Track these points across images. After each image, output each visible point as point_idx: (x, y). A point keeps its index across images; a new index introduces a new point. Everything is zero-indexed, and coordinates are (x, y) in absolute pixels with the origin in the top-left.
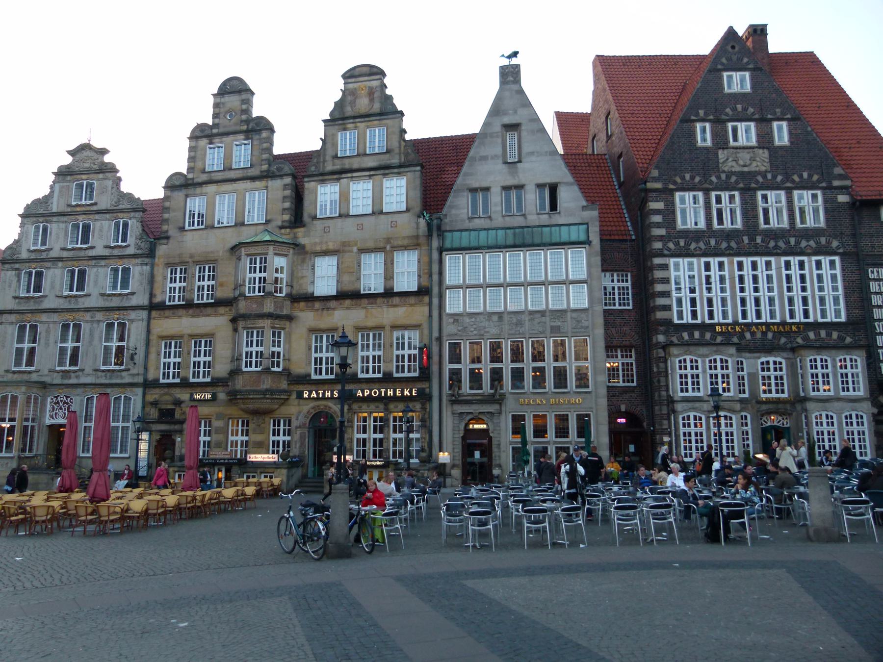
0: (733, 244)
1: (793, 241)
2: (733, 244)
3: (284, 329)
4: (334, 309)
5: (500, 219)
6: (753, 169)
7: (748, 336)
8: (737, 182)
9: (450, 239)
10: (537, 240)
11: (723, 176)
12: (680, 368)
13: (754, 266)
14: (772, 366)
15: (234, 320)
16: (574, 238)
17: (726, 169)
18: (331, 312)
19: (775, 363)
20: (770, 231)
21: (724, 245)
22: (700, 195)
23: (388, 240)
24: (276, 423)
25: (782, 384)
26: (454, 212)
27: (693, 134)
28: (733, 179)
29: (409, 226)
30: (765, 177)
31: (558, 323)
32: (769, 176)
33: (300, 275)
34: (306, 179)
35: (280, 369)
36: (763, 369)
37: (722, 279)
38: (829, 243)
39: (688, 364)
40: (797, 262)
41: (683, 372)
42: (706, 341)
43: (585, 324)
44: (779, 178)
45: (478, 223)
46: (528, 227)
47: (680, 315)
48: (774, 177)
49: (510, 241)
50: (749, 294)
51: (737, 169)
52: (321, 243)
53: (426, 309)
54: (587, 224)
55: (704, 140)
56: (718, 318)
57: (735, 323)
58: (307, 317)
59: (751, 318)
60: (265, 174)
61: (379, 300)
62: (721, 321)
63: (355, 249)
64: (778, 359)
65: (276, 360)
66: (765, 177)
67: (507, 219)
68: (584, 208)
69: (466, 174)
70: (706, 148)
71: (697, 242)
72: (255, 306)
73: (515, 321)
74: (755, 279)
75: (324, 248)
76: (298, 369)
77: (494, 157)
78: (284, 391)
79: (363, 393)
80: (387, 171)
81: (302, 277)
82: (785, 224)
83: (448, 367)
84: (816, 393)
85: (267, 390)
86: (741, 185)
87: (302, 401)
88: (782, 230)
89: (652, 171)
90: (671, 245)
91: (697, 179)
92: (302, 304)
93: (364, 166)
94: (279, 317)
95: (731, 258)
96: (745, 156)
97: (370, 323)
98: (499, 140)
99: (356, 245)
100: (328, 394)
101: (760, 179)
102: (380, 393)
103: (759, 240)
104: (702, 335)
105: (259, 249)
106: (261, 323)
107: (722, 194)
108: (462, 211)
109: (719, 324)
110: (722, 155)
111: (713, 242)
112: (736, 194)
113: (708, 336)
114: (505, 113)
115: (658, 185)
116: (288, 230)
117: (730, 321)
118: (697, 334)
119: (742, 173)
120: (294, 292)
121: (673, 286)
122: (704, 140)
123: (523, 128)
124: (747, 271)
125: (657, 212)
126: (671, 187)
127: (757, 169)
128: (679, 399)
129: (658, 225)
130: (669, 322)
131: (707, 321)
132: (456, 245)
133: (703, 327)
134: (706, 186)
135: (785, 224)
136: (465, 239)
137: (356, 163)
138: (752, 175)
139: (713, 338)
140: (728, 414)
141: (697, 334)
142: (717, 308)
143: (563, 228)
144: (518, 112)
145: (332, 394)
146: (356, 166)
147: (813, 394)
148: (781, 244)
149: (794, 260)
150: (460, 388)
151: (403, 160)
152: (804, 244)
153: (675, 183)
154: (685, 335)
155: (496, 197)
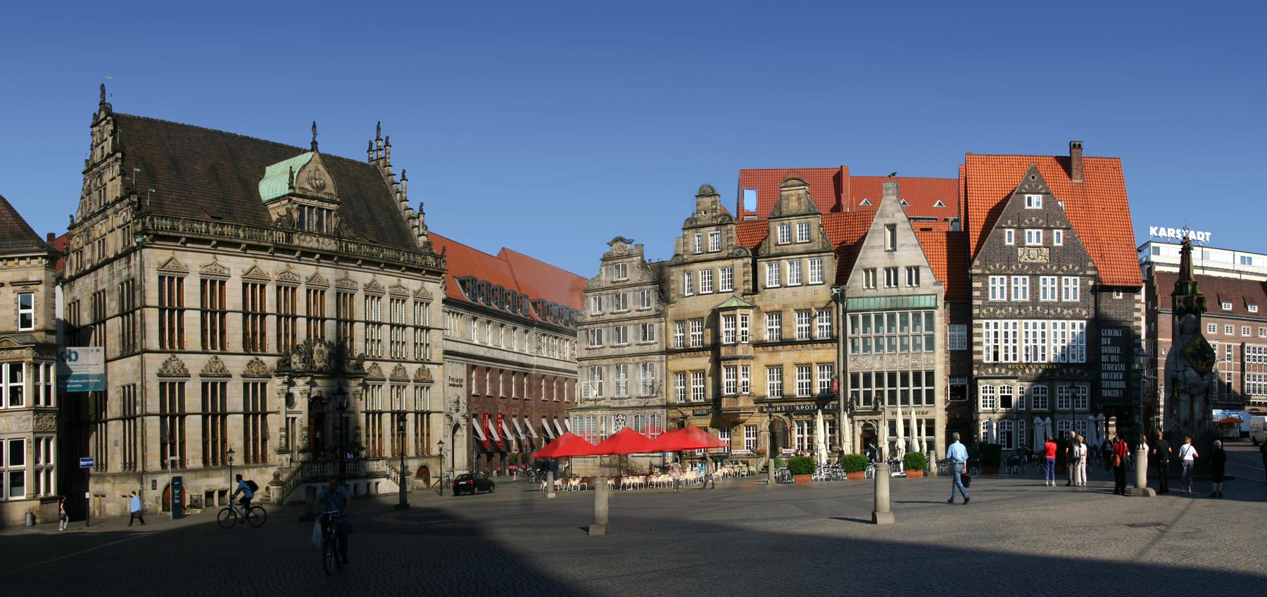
0: (1023, 311)
1: (1059, 310)
2: (1023, 311)
3: (749, 365)
4: (780, 351)
5: (883, 290)
6: (1039, 260)
7: (1027, 371)
8: (1028, 270)
9: (851, 304)
10: (905, 306)
11: (1020, 266)
12: (983, 392)
13: (1035, 325)
14: (1040, 390)
15: (717, 361)
16: (927, 304)
17: (1022, 260)
18: (778, 353)
19: (1042, 388)
20: (1047, 303)
21: (1017, 312)
22: (1005, 277)
23: (812, 303)
24: (748, 428)
25: (1045, 402)
26: (854, 284)
27: (1002, 237)
28: (1026, 267)
29: (824, 294)
30: (1045, 267)
31: (916, 361)
32: (1048, 266)
33: (758, 327)
34: (758, 260)
35: (748, 393)
36: (1035, 393)
37: (1015, 333)
38: (1080, 311)
39: (988, 390)
40: (1060, 324)
41: (985, 394)
42: (1002, 374)
43: (932, 362)
44: (1055, 268)
45: (869, 292)
46: (900, 296)
47: (988, 359)
48: (1051, 267)
49: (888, 307)
50: (1031, 343)
51: (1029, 261)
52: (770, 305)
53: (836, 350)
54: (936, 295)
55: (1010, 240)
56: (1011, 360)
57: (1021, 363)
58: (765, 357)
59: (1031, 359)
60: (730, 256)
61: (809, 345)
62: (1013, 362)
63: (792, 310)
64: (1044, 386)
65: (745, 386)
66: (1045, 267)
67: (887, 290)
68: (935, 284)
69: (861, 259)
70: (1011, 247)
71: (1001, 309)
72: (730, 351)
73: (890, 360)
74: (1035, 334)
75: (772, 309)
76: (759, 393)
77: (880, 247)
78: (753, 408)
79: (800, 408)
80: (811, 255)
81: (759, 329)
82: (1056, 300)
83: (850, 390)
84: (1061, 409)
85: (741, 408)
86: (1031, 272)
87: (763, 414)
88: (1053, 302)
89: (976, 261)
90: (985, 311)
91: (1004, 267)
92: (760, 348)
93: (796, 251)
94: (745, 358)
95: (1020, 320)
96: (1034, 252)
97: (803, 361)
98: (883, 235)
99: (792, 307)
100: (779, 409)
101: (1042, 268)
102: (810, 407)
103: (1039, 308)
104: (1000, 371)
105: (731, 312)
106: (734, 363)
107: (1018, 277)
108: (859, 284)
109: (1011, 364)
110: (1020, 251)
111: (1010, 309)
112: (1027, 277)
113: (1003, 371)
114: (887, 217)
115: (979, 271)
116: (749, 296)
117: (1017, 361)
118: (997, 370)
119: (1032, 264)
120: (754, 340)
121: (984, 338)
122: (1010, 240)
123: (898, 227)
124: (1031, 330)
125: (978, 289)
126: (987, 272)
127: (1042, 261)
128: (981, 412)
129: (978, 298)
130: (980, 362)
131: (1004, 361)
132: (855, 308)
133: (1001, 365)
134: (1009, 272)
135: (1056, 300)
136: (860, 304)
137: (790, 248)
138: (1038, 265)
139: (1007, 372)
140: (1010, 421)
141: (997, 370)
142: (1011, 354)
143: (921, 297)
144: (895, 216)
145: (781, 409)
146: (790, 251)
147: (1058, 408)
148: (1052, 312)
149: (1059, 322)
150: (858, 404)
151: (821, 248)
152: (1065, 312)
153: (989, 270)
154: (990, 370)
155: (882, 275)
